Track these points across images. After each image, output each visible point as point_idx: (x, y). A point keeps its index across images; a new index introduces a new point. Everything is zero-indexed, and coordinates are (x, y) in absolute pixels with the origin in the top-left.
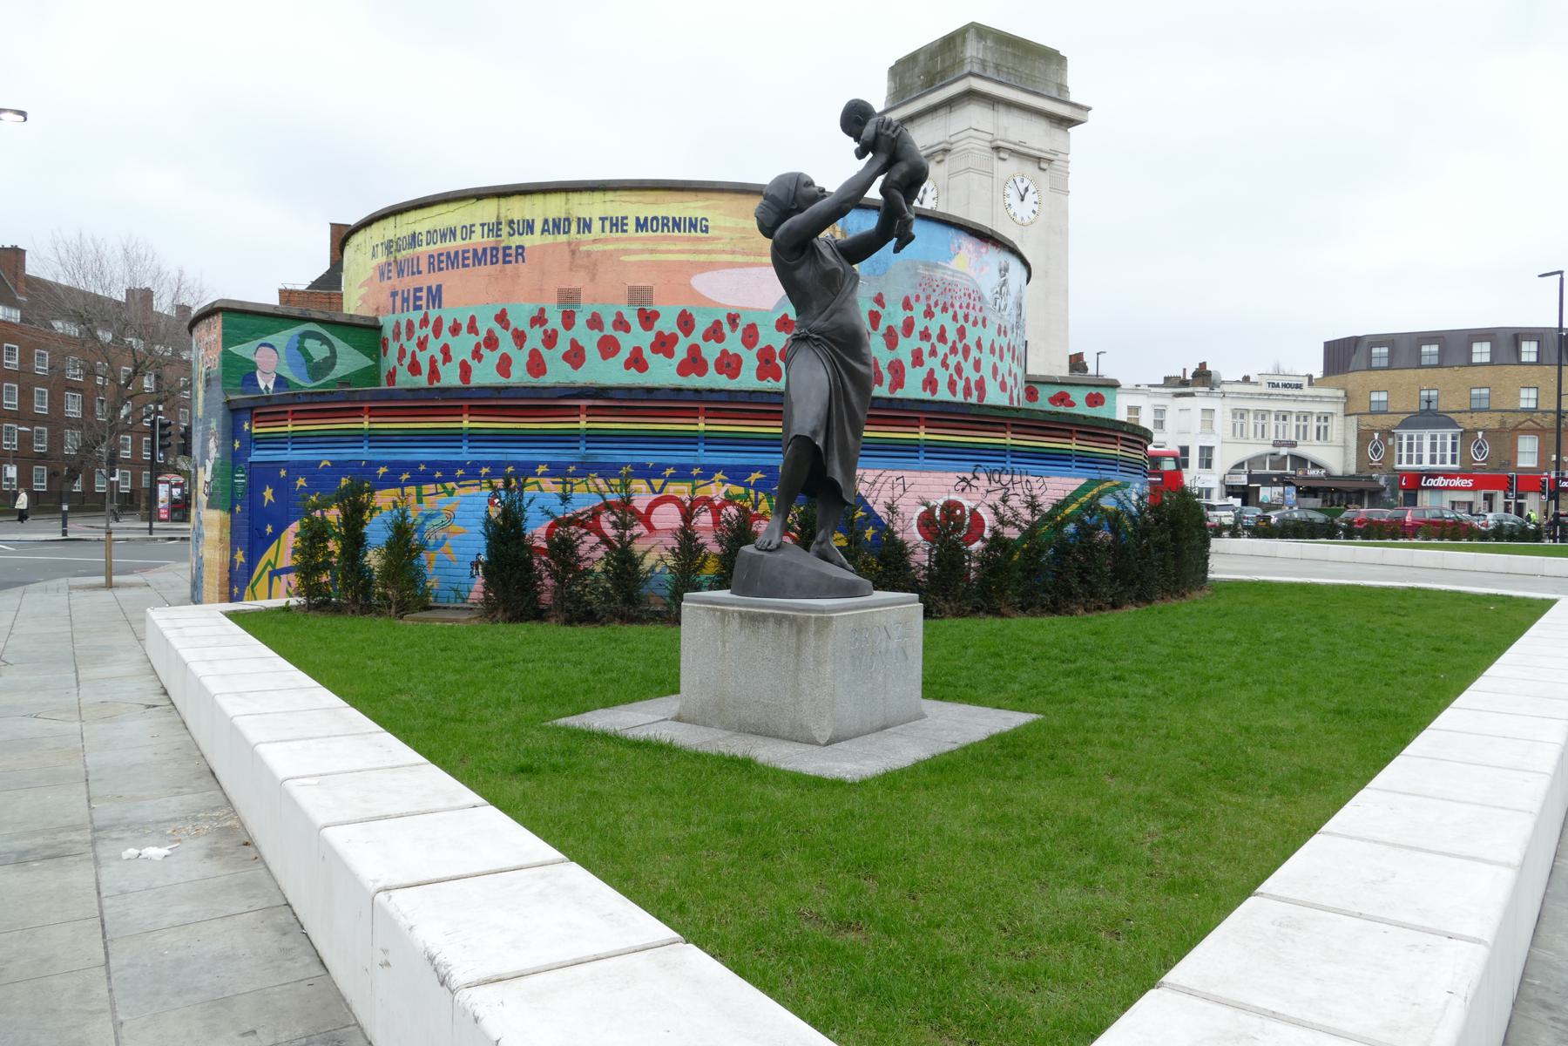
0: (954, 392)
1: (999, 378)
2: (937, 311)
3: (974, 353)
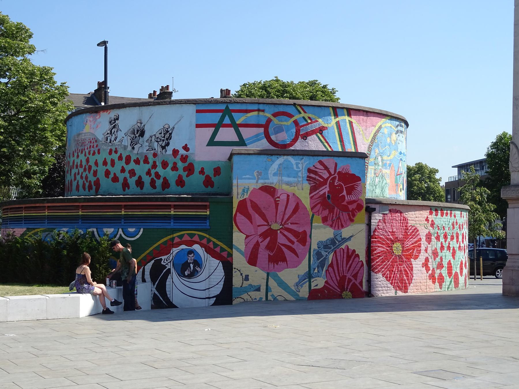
3: (94, 168)
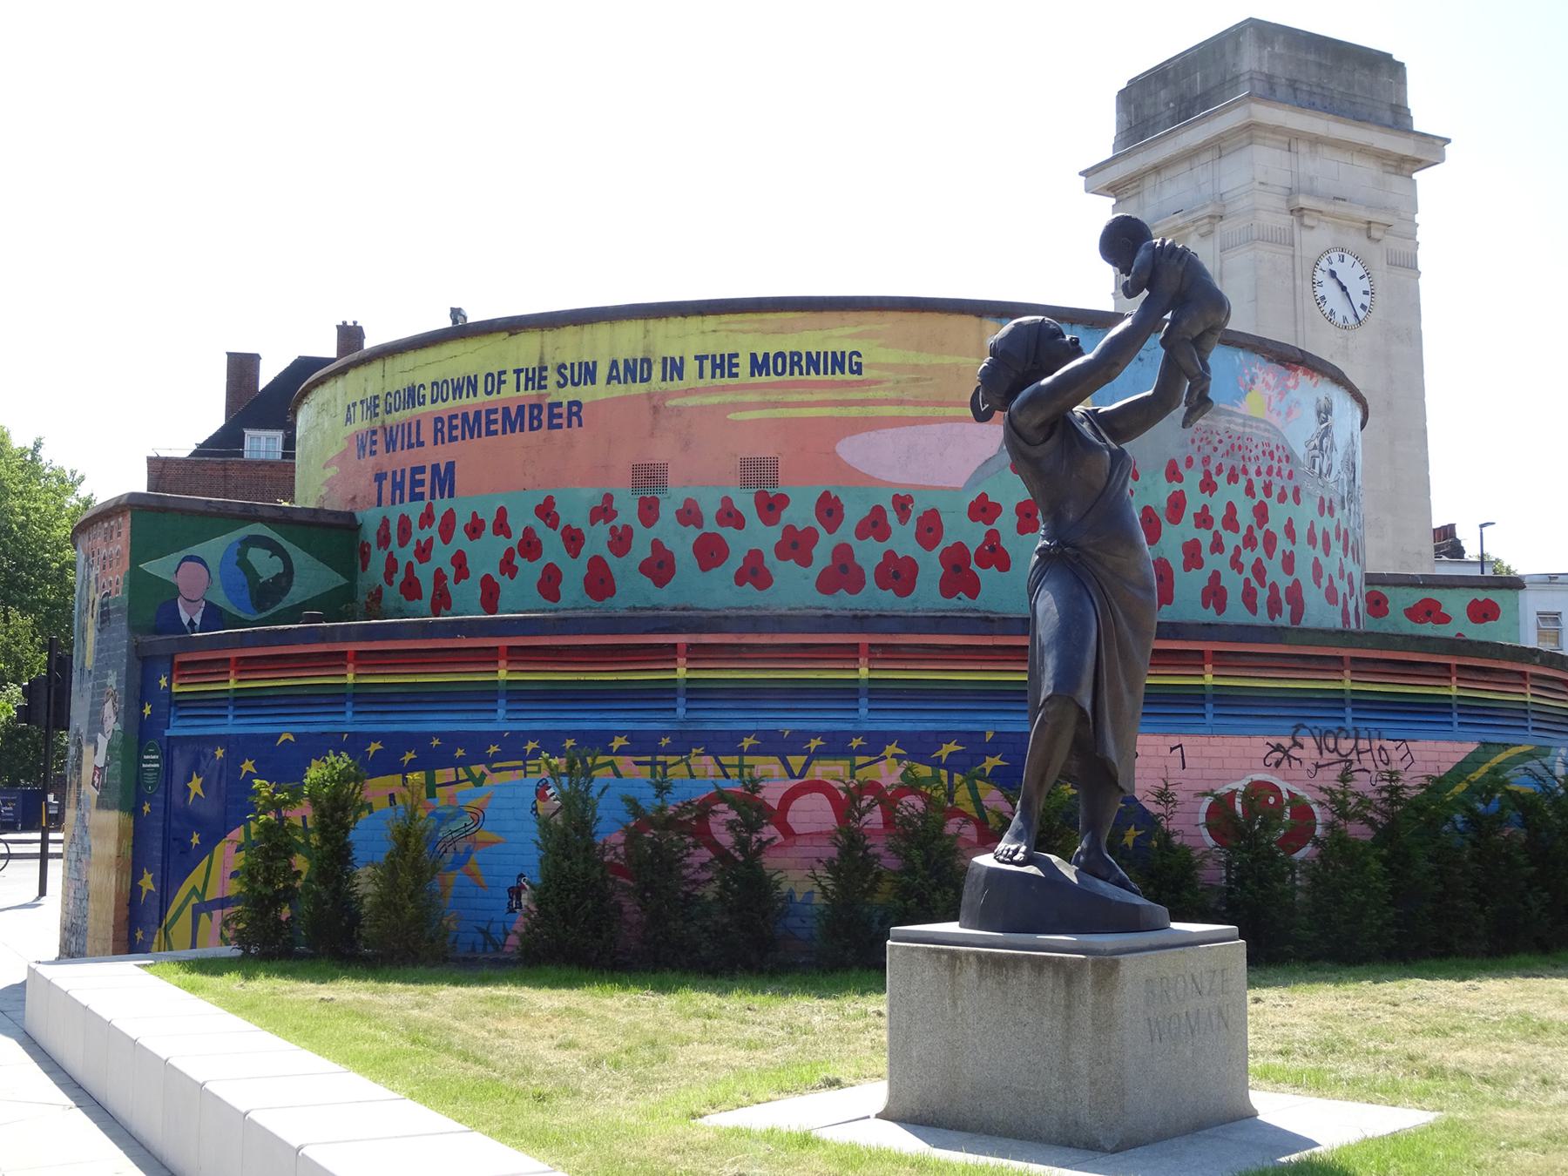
0: (1253, 609)
1: (1325, 582)
2: (1220, 481)
3: (1283, 544)
